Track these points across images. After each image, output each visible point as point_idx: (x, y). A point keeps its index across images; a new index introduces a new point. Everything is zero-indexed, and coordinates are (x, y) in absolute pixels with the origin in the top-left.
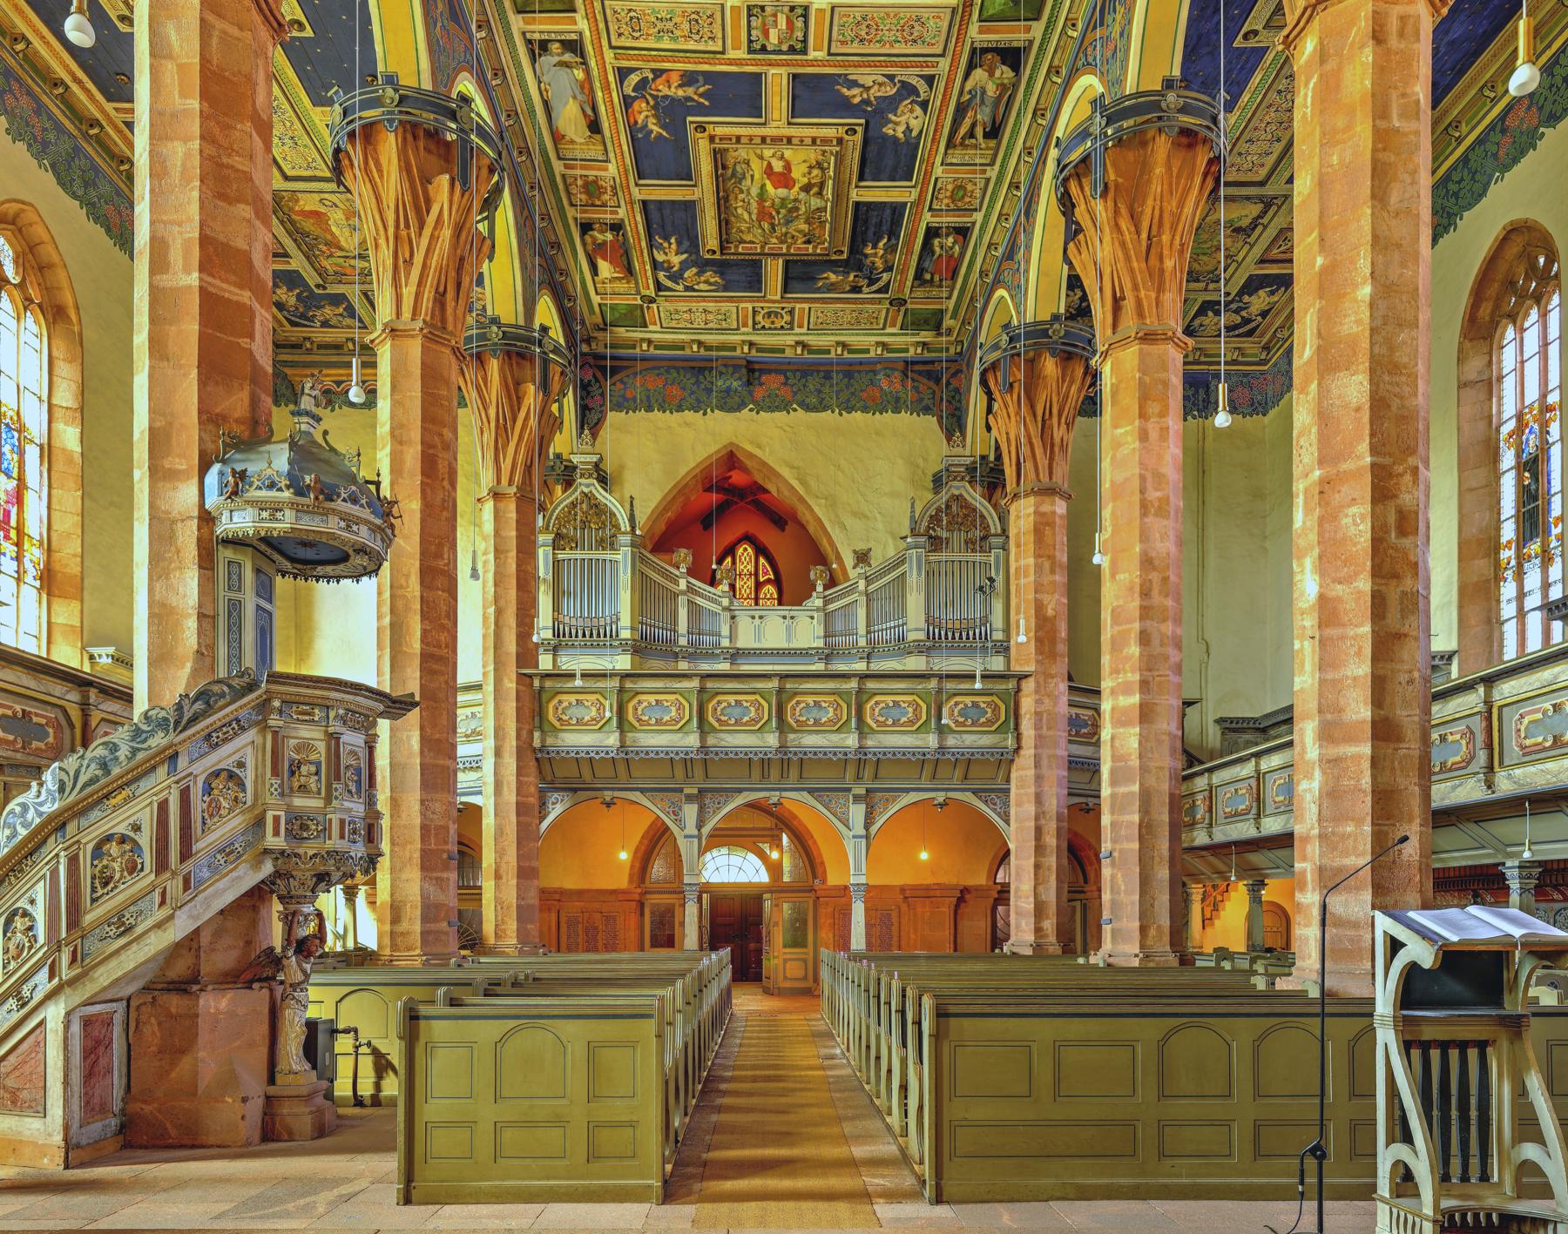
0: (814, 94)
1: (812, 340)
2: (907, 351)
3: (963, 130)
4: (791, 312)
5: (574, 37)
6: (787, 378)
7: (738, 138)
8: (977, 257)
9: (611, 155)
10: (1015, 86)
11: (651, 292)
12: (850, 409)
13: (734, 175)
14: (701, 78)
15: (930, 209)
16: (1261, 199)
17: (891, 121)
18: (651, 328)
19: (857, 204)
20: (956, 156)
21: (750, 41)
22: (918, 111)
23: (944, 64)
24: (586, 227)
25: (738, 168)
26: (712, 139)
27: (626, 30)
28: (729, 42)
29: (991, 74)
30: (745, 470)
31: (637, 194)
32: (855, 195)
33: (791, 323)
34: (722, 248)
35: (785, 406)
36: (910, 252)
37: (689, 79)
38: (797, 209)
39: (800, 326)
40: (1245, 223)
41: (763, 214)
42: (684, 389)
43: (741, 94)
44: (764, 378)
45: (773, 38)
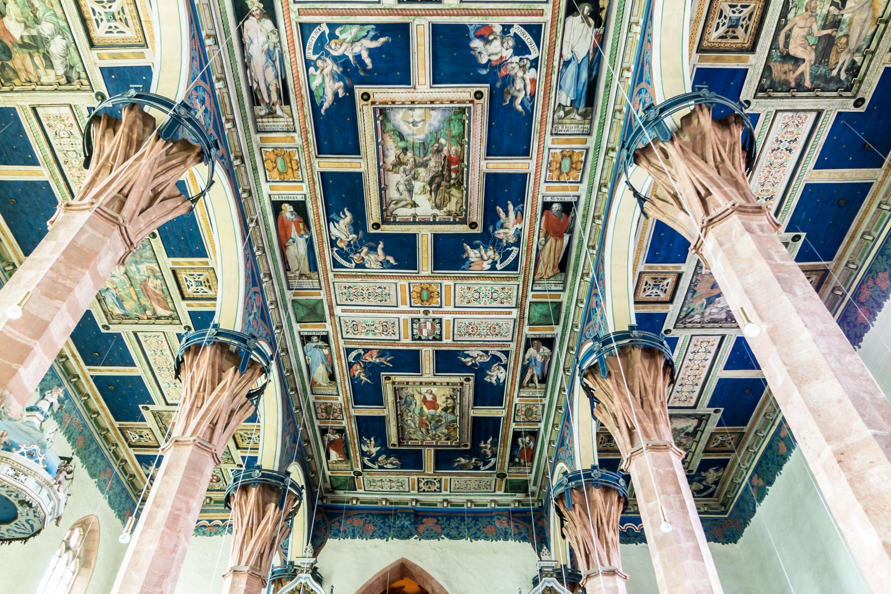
0: (448, 361)
1: (454, 499)
2: (508, 505)
3: (527, 378)
4: (440, 481)
5: (324, 334)
6: (438, 520)
7: (408, 383)
8: (544, 451)
9: (340, 392)
10: (551, 357)
11: (359, 469)
12: (477, 538)
13: (406, 402)
14: (388, 354)
15: (514, 421)
16: (695, 416)
17: (488, 375)
18: (359, 491)
19: (474, 418)
20: (525, 392)
21: (413, 335)
22: (502, 369)
23: (513, 346)
24: (324, 431)
26: (394, 383)
27: (351, 330)
28: (402, 335)
29: (538, 351)
30: (412, 577)
31: (353, 413)
32: (473, 413)
33: (440, 488)
34: (399, 442)
35: (437, 536)
36: (505, 446)
37: (382, 353)
38: (441, 421)
39: (446, 490)
40: (691, 430)
41: (422, 424)
42: (375, 526)
43: (408, 361)
44: (424, 520)
45: (425, 333)
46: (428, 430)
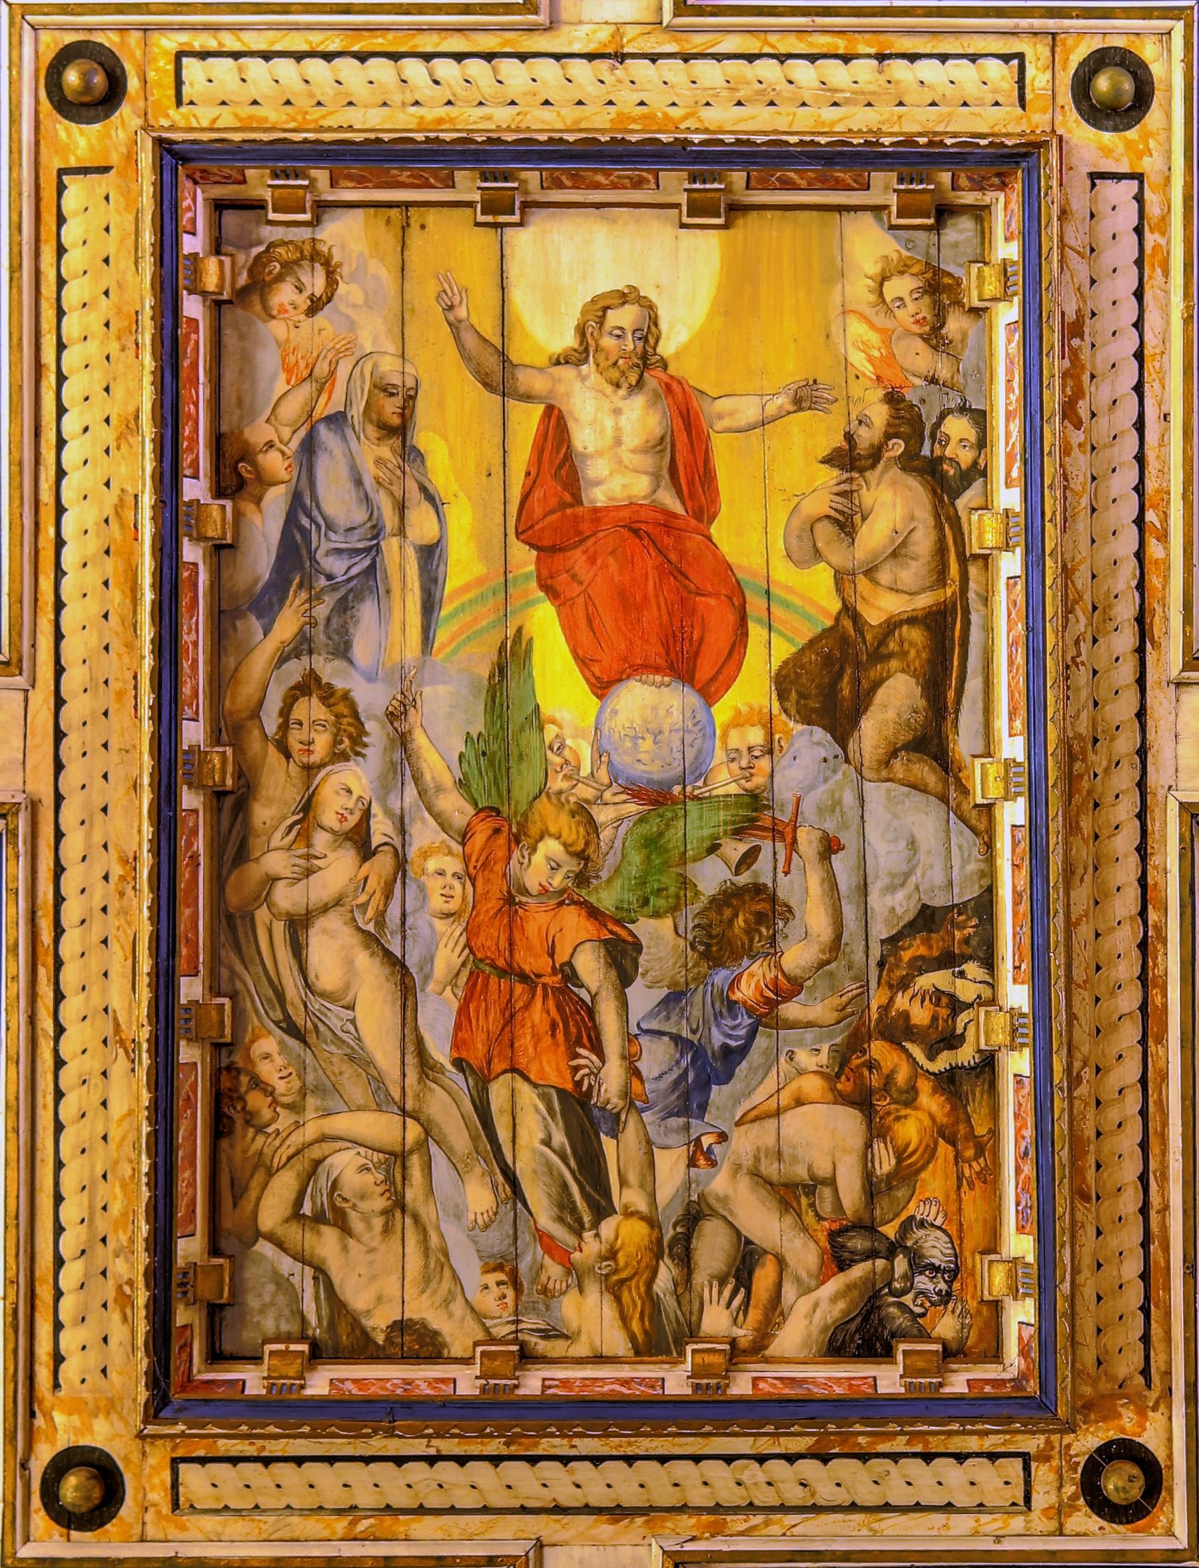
13: (294, 555)
25: (336, 499)
38: (745, 919)
46: (583, 1118)
